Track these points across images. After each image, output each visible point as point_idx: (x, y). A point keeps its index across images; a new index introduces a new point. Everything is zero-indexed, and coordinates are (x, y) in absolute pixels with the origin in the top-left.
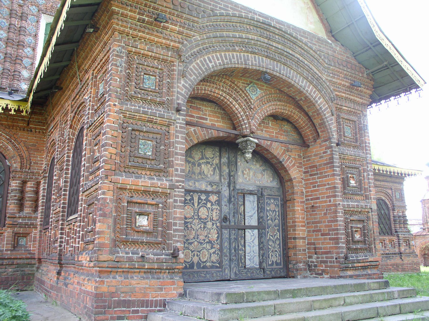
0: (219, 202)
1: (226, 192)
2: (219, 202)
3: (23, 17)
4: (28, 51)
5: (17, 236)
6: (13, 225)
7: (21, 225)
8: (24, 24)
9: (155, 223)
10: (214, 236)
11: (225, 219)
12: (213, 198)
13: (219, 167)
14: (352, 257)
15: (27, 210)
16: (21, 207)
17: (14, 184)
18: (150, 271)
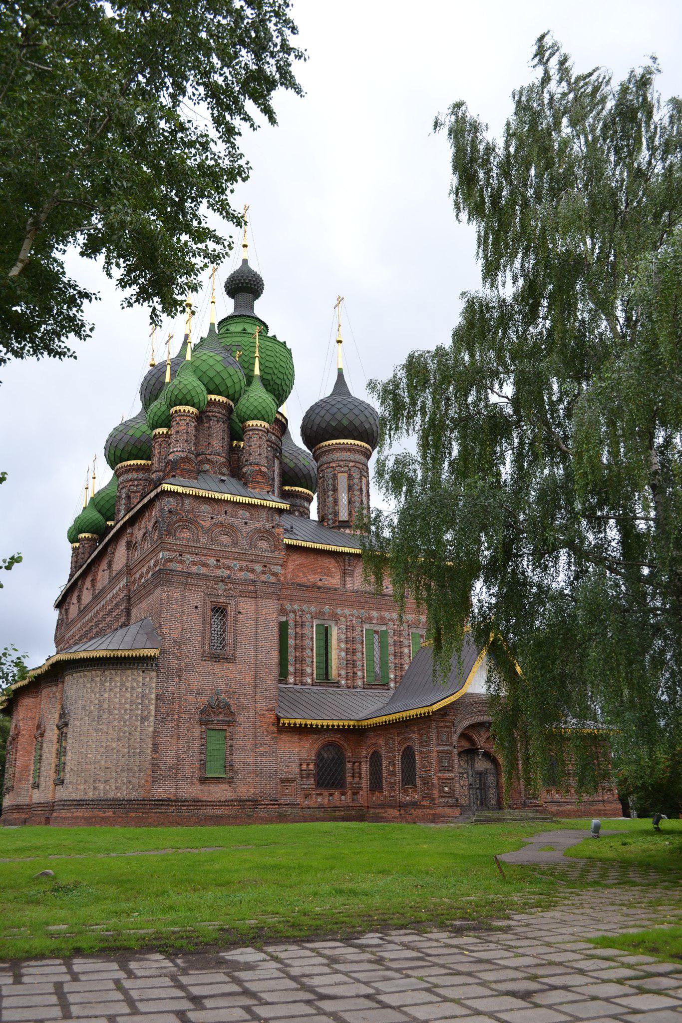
0: (468, 777)
1: (470, 773)
2: (468, 777)
3: (302, 626)
4: (308, 651)
5: (354, 794)
6: (352, 789)
7: (355, 788)
8: (304, 631)
9: (450, 790)
10: (466, 792)
11: (471, 785)
12: (465, 775)
13: (467, 761)
14: (528, 801)
15: (356, 780)
16: (353, 777)
17: (349, 765)
18: (450, 806)
